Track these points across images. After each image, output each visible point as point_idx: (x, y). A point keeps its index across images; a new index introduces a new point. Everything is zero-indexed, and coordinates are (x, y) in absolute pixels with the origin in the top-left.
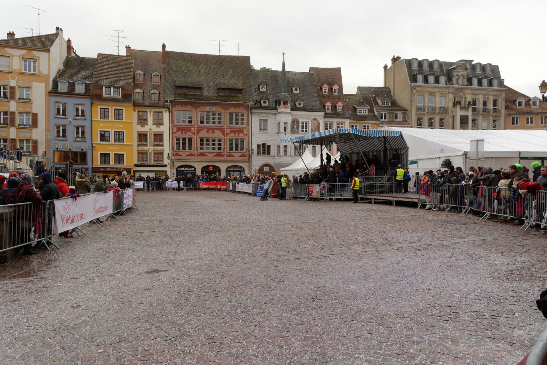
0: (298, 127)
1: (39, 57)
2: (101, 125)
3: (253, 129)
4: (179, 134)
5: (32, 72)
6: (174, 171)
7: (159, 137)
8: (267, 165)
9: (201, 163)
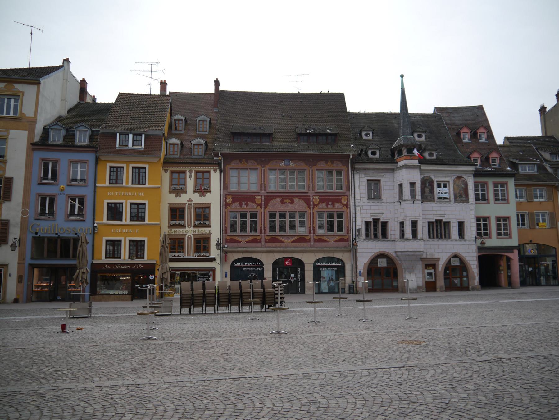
1: (23, 93)
2: (109, 193)
3: (357, 195)
5: (11, 114)
6: (228, 269)
8: (382, 255)
9: (271, 254)
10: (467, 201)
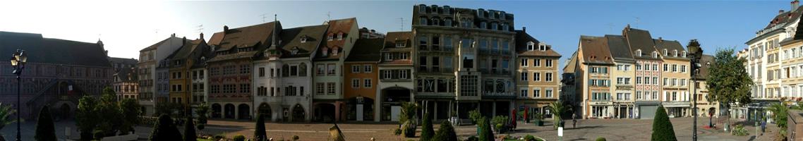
0: (288, 72)
4: (212, 83)
7: (202, 86)
10: (306, 75)
